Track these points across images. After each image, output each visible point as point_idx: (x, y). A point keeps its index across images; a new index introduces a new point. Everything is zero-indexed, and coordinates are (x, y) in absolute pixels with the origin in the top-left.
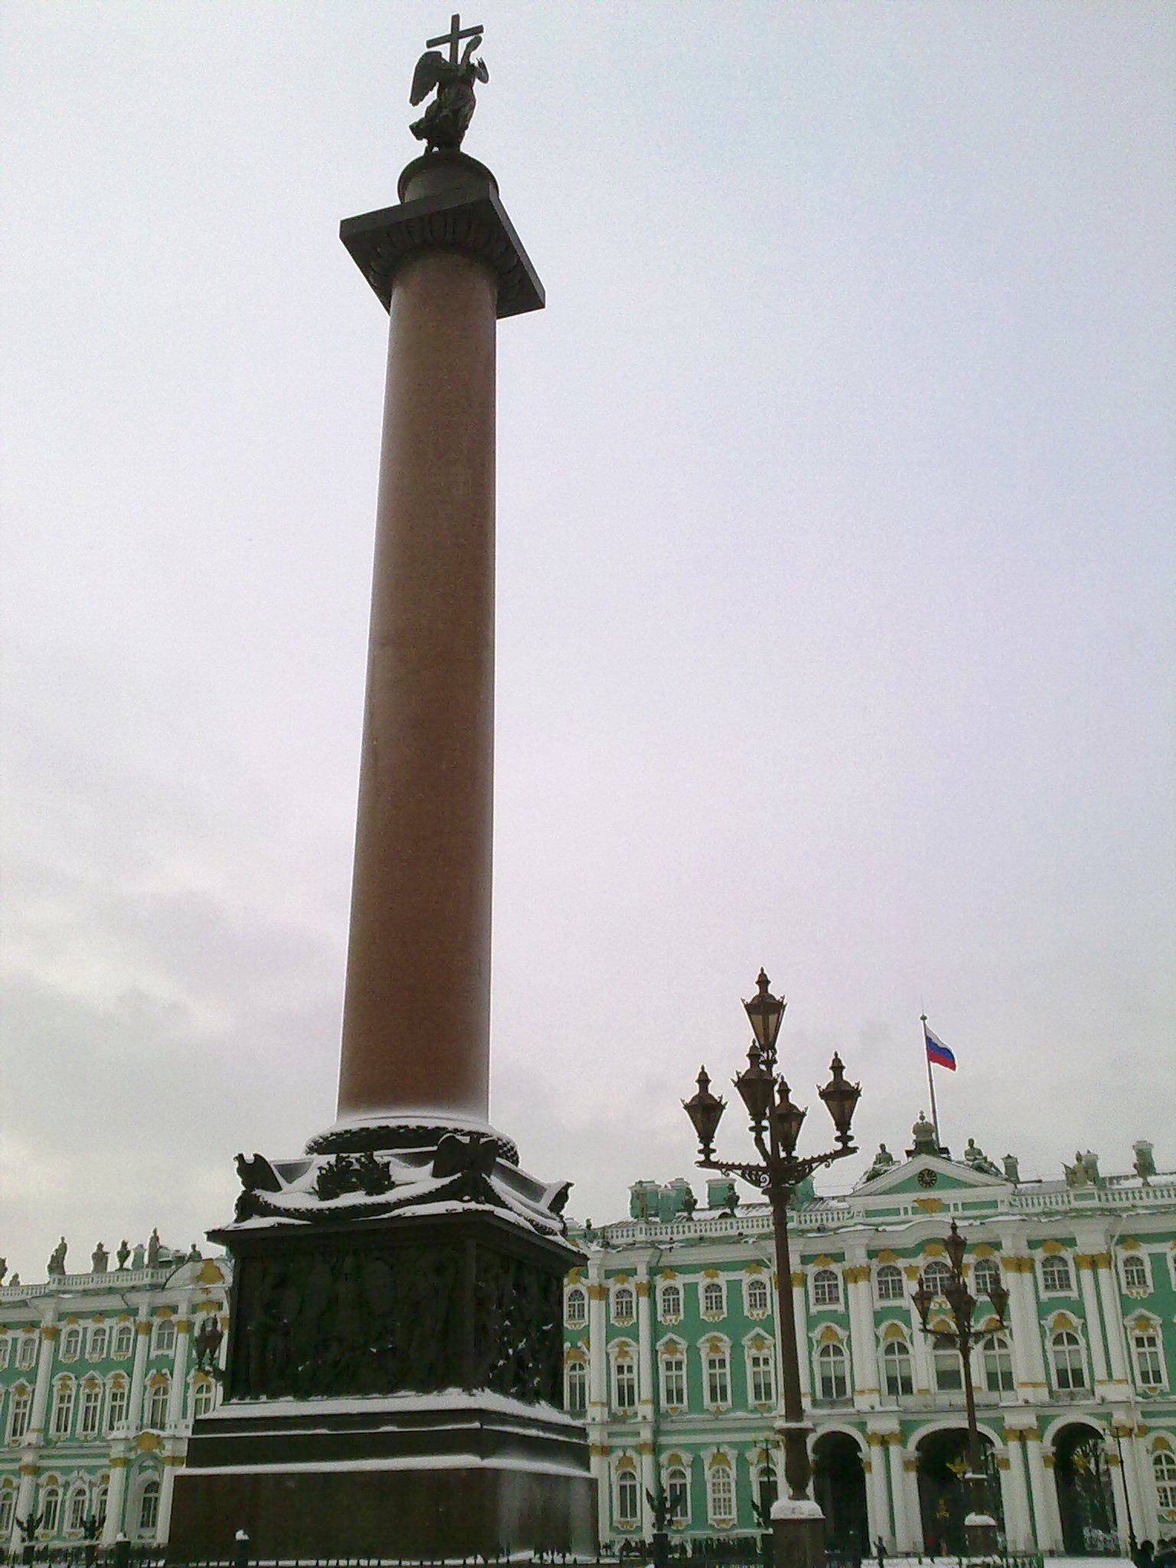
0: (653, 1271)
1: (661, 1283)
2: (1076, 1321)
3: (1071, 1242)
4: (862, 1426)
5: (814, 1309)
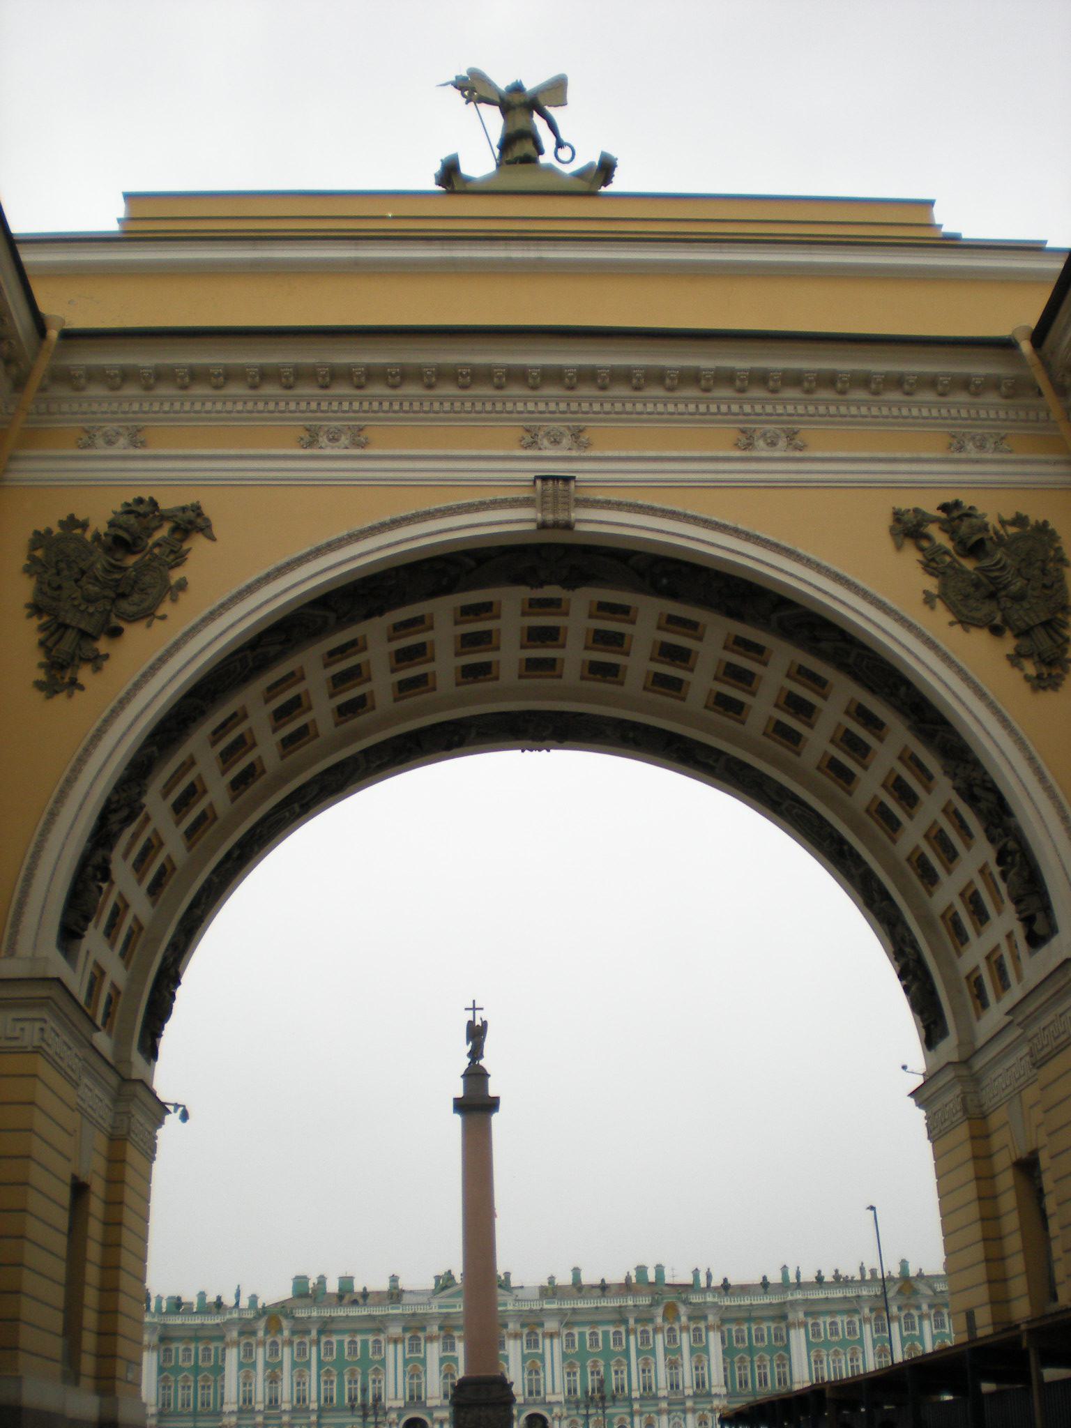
0: (320, 1332)
1: (324, 1339)
2: (539, 1363)
3: (542, 1325)
4: (431, 1415)
5: (407, 1356)
